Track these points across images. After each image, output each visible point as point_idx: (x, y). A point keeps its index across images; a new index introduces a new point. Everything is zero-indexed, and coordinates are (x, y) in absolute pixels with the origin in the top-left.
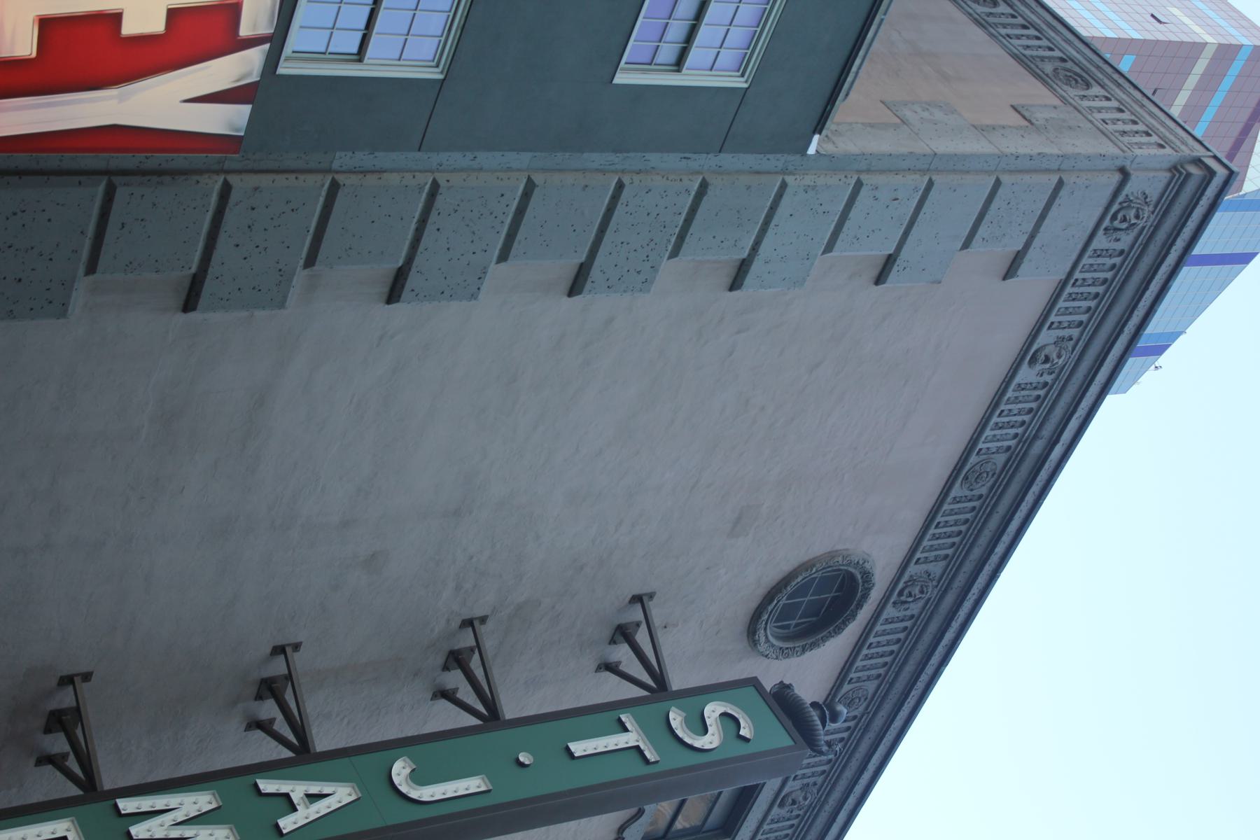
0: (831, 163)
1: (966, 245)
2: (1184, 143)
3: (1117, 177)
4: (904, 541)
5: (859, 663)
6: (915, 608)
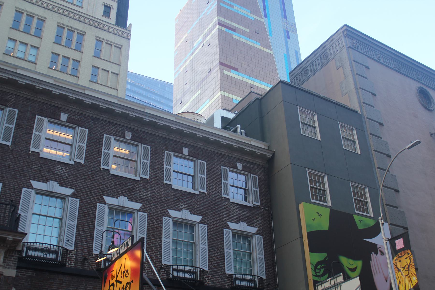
0: (361, 108)
1: (366, 78)
2: (339, 34)
3: (350, 49)
4: (412, 82)
5: (432, 86)
6: (358, 45)
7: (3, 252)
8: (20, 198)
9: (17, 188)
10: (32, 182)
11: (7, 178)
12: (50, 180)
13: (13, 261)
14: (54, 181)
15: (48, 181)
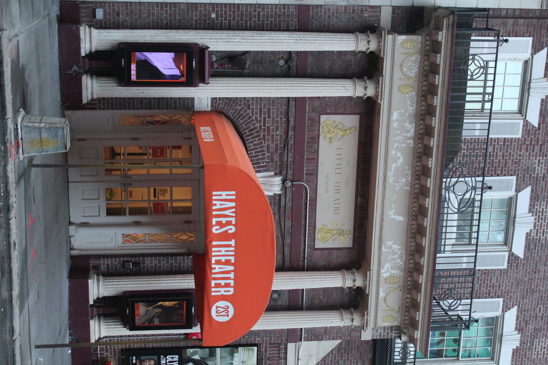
7: (396, 324)
8: (486, 298)
9: (502, 290)
10: (514, 311)
11: (517, 273)
12: (522, 333)
13: (384, 332)
14: (521, 341)
15: (519, 331)
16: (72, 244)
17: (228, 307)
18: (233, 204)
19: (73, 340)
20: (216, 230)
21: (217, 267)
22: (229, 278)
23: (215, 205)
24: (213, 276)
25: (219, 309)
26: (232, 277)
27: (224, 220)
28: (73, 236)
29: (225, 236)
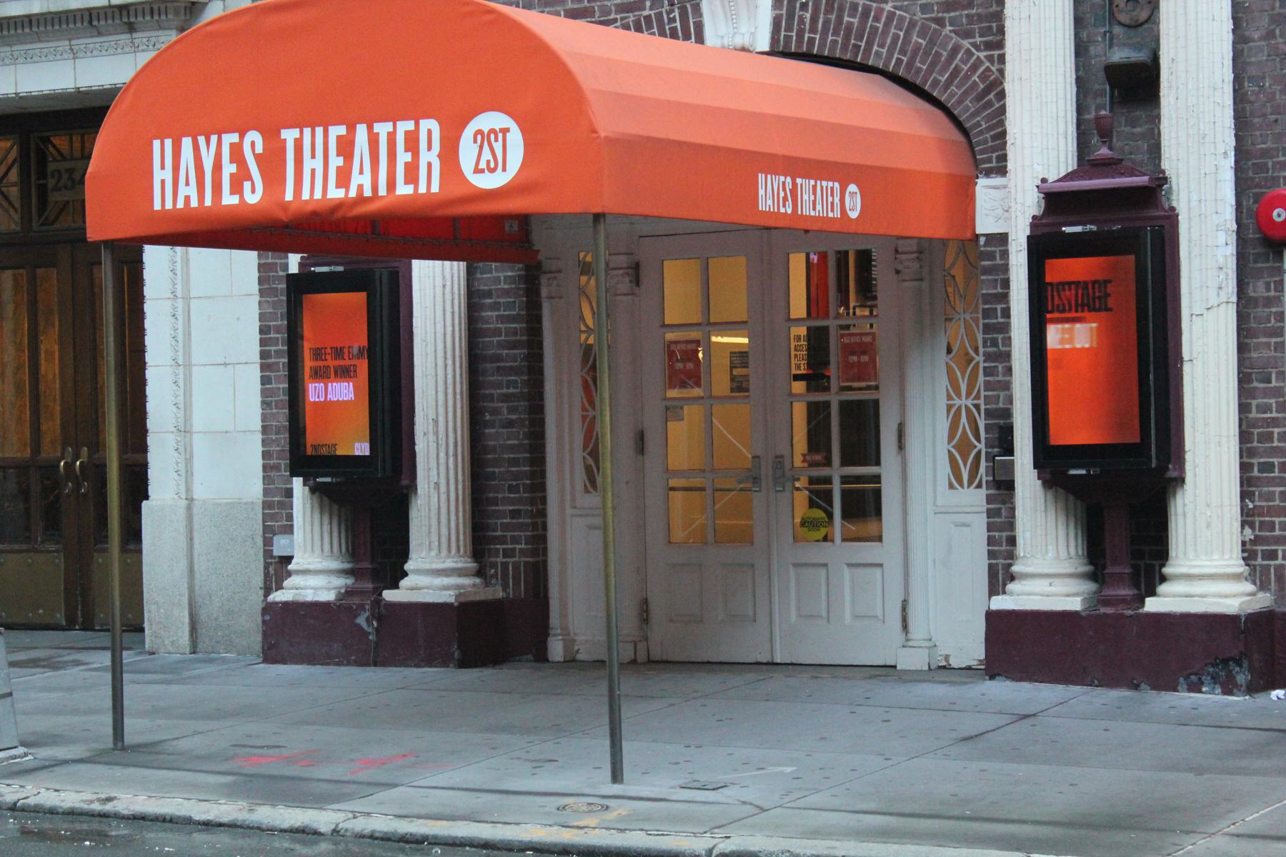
16: (973, 663)
17: (480, 132)
18: (187, 142)
19: (1215, 679)
20: (253, 191)
21: (356, 180)
22: (392, 137)
23: (187, 199)
24: (382, 191)
25: (483, 165)
26: (388, 127)
27: (229, 169)
28: (947, 657)
29: (272, 163)
